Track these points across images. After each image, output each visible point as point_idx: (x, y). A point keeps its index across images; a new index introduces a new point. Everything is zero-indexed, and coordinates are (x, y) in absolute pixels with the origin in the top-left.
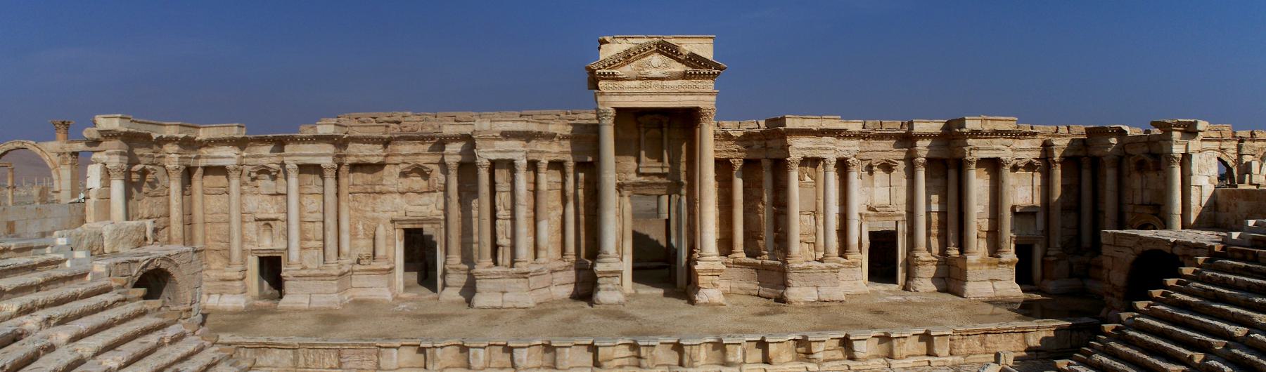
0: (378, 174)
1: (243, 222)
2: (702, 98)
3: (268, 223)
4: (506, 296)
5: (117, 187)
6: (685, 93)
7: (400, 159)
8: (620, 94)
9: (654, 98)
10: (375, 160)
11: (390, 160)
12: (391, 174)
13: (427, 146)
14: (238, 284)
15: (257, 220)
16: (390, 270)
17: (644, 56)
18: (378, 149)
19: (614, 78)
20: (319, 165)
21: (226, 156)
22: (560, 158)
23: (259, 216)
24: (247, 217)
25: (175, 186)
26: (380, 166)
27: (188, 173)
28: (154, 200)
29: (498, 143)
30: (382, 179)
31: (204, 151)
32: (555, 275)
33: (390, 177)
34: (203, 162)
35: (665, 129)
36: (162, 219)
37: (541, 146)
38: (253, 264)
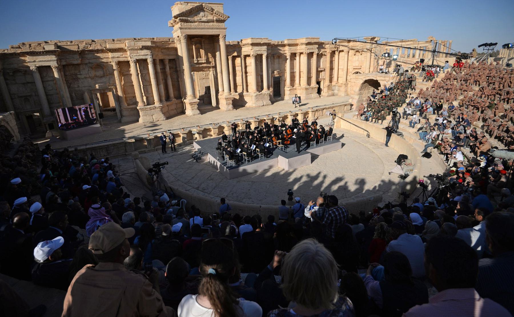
1: (12, 99)
2: (221, 30)
3: (26, 99)
6: (215, 28)
8: (189, 28)
9: (203, 30)
10: (76, 62)
15: (21, 97)
17: (198, 11)
19: (187, 21)
20: (49, 66)
22: (162, 58)
26: (78, 65)
29: (139, 51)
35: (203, 44)
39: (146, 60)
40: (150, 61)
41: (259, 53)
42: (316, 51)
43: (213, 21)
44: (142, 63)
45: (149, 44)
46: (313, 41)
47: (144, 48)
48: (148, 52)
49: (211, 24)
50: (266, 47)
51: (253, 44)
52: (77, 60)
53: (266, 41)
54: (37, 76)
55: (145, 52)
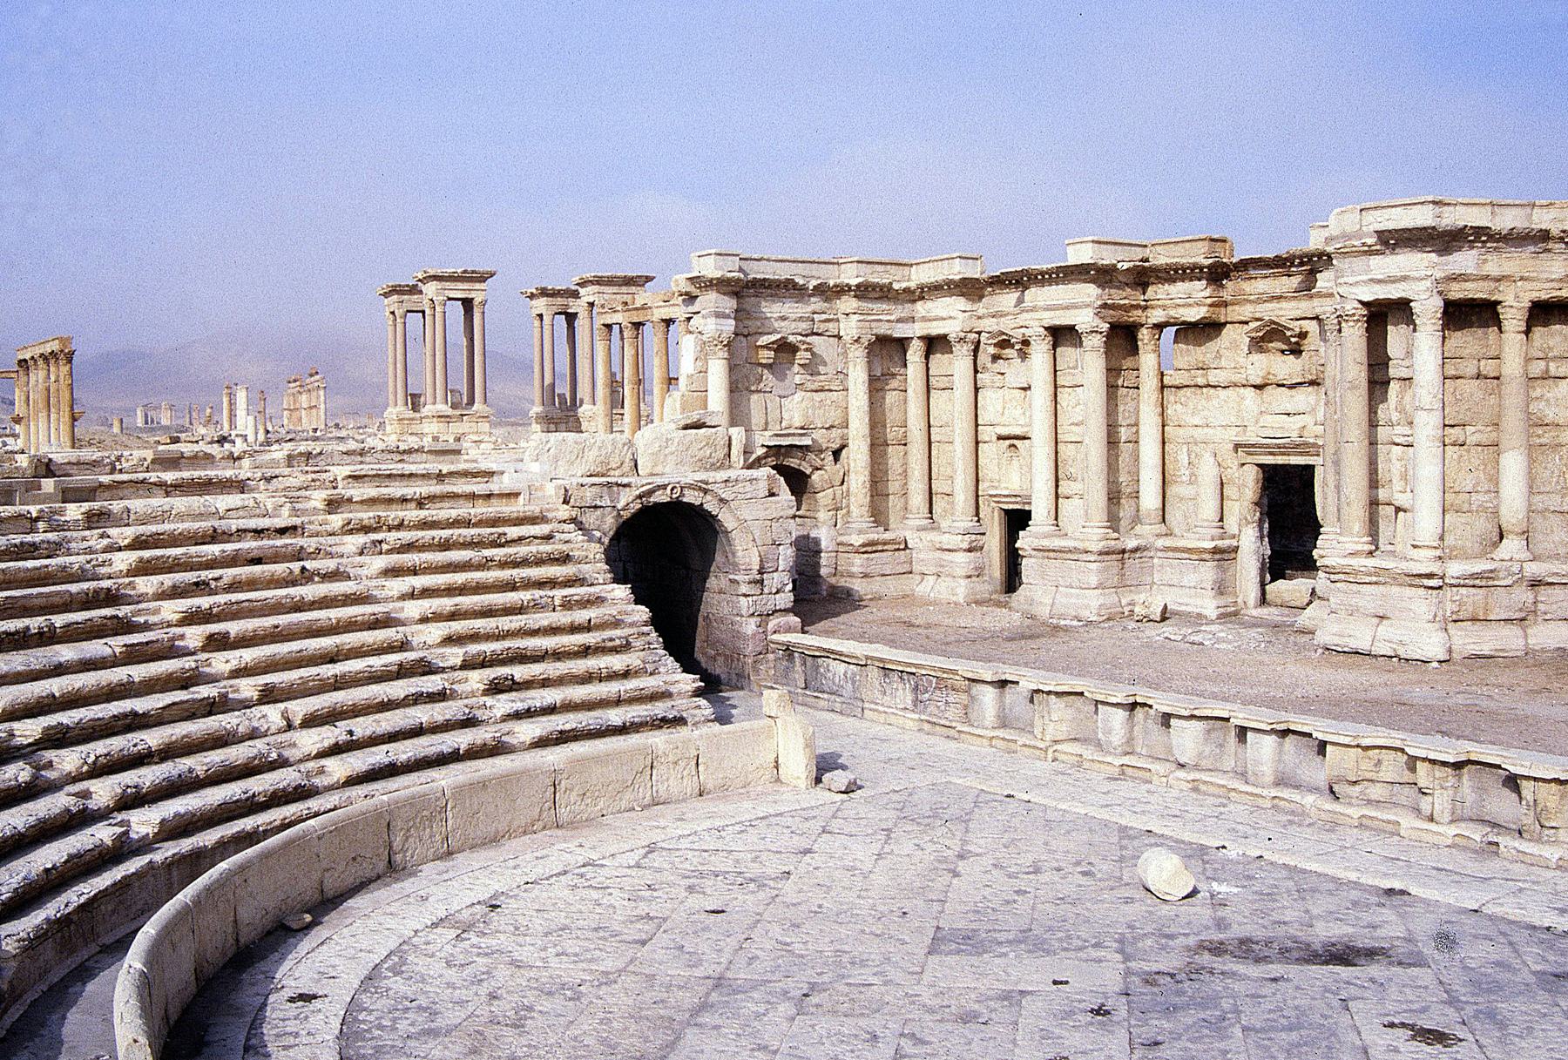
0: (1212, 346)
4: (1384, 630)
5: (717, 371)
7: (1246, 311)
11: (1234, 313)
12: (1235, 345)
13: (1295, 281)
14: (961, 557)
15: (1000, 438)
16: (1224, 555)
18: (1199, 289)
21: (948, 316)
23: (1004, 431)
24: (986, 433)
25: (858, 376)
27: (887, 349)
28: (818, 396)
29: (1375, 261)
30: (1219, 356)
31: (921, 308)
32: (1544, 593)
33: (1230, 351)
34: (919, 329)
36: (835, 433)
37: (1497, 263)
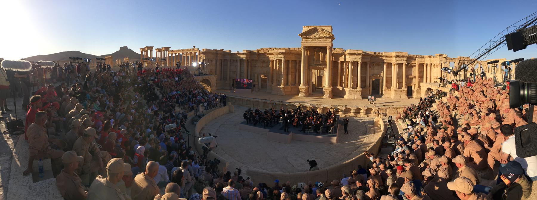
38: (232, 80)
39: (281, 60)
40: (283, 60)
41: (355, 60)
42: (405, 63)
43: (322, 38)
44: (280, 61)
45: (284, 51)
46: (401, 55)
47: (281, 53)
48: (282, 56)
49: (321, 39)
50: (361, 56)
51: (396, 57)
52: (256, 58)
53: (406, 55)
54: (239, 63)
55: (281, 56)
